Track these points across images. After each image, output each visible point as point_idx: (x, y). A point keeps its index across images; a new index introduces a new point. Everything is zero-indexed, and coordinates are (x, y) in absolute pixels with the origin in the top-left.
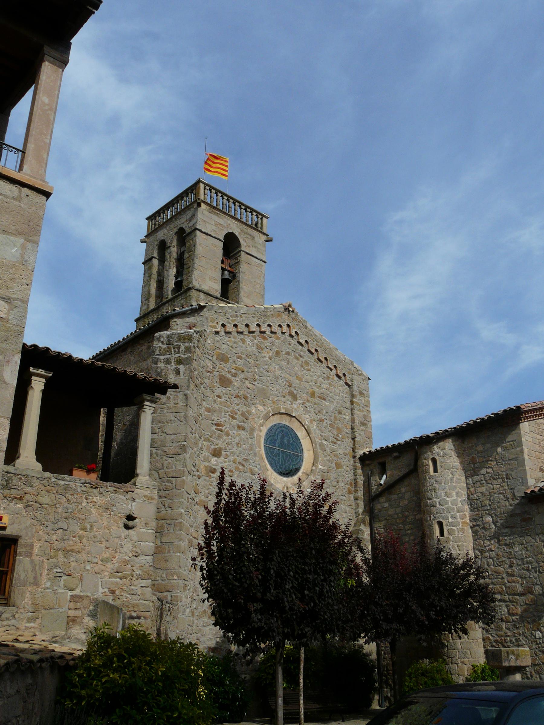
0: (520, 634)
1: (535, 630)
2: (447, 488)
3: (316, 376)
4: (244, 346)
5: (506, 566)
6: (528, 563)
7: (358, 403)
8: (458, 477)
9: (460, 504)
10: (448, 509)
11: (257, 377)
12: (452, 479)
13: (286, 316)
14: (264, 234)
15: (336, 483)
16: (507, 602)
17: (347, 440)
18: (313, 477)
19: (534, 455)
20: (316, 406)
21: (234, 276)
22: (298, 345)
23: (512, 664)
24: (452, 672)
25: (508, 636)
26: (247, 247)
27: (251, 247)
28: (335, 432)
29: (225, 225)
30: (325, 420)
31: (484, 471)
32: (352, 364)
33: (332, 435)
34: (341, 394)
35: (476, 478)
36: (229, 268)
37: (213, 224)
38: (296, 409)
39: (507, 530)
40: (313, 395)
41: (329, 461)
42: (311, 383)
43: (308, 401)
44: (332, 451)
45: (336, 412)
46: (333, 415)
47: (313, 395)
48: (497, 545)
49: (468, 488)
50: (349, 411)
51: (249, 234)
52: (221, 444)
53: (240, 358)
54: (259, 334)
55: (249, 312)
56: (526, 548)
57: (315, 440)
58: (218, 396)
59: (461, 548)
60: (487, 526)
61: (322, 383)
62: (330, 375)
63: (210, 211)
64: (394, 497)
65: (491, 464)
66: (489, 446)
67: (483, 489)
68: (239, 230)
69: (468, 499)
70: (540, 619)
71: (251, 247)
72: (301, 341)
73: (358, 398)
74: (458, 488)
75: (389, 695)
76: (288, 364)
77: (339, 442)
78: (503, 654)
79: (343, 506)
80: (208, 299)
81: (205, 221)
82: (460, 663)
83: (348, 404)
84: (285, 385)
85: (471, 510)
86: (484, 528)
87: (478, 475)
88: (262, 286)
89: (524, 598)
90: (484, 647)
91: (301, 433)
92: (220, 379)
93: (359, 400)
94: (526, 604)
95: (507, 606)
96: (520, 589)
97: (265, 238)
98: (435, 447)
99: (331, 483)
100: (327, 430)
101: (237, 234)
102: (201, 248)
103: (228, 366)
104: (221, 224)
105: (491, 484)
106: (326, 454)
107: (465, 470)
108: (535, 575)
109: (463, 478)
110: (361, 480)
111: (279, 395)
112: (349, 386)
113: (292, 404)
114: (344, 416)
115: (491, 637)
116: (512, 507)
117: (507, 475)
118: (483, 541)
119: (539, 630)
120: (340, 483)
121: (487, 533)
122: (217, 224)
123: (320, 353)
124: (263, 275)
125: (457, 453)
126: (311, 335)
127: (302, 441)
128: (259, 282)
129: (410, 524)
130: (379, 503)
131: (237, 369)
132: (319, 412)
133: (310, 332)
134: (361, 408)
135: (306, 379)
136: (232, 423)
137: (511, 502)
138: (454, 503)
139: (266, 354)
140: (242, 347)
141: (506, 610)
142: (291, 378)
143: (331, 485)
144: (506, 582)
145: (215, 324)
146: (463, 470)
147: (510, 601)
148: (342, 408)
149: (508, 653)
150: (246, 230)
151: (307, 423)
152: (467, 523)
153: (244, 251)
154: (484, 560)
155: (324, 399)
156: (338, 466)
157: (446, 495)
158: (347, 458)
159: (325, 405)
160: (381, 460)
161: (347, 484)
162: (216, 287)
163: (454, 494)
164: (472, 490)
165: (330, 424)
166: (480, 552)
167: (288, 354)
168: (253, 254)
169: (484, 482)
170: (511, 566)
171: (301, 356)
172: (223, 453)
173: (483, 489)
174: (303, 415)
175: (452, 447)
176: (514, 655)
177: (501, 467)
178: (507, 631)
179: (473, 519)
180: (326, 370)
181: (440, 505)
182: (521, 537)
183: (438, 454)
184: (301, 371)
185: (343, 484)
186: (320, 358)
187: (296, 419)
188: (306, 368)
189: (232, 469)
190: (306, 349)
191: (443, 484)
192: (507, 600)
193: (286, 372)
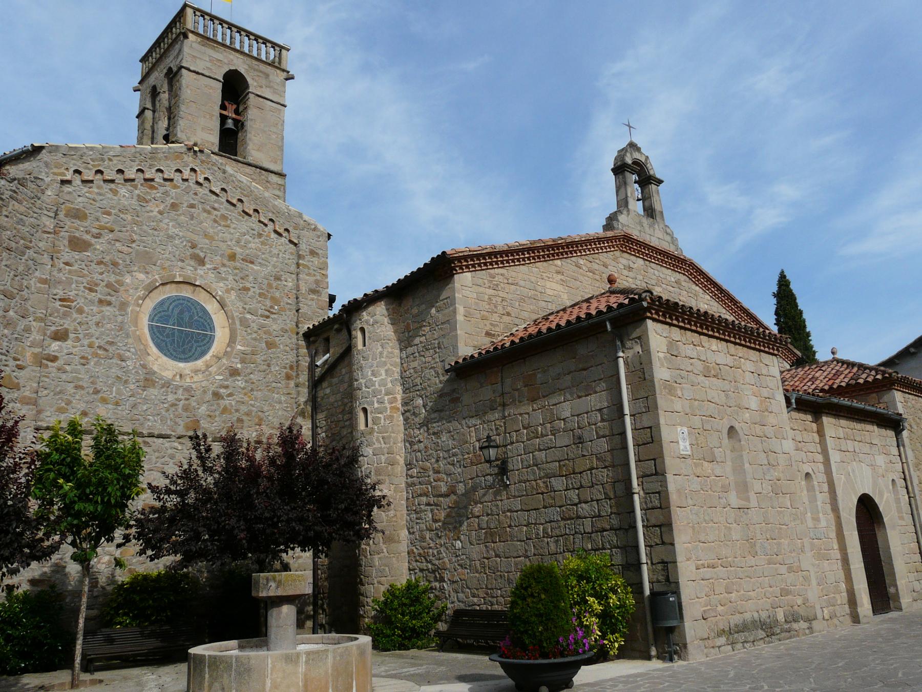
0: (441, 546)
1: (455, 540)
2: (375, 365)
3: (238, 234)
4: (115, 198)
5: (433, 460)
6: (453, 455)
7: (305, 266)
8: (390, 350)
9: (390, 385)
10: (374, 391)
11: (135, 237)
12: (381, 353)
13: (191, 158)
14: (284, 70)
15: (265, 367)
16: (432, 505)
17: (288, 313)
18: (227, 360)
19: (479, 316)
20: (237, 271)
21: (240, 125)
22: (210, 194)
23: (271, 594)
24: (368, 594)
25: (430, 548)
26: (259, 88)
28: (268, 303)
29: (226, 61)
30: (252, 289)
31: (417, 340)
32: (300, 215)
33: (263, 308)
34: (280, 255)
35: (410, 350)
36: (234, 116)
37: (208, 60)
38: (203, 275)
39: (436, 415)
40: (232, 257)
41: (255, 339)
42: (229, 243)
43: (224, 265)
44: (262, 327)
45: (272, 278)
46: (266, 282)
47: (232, 257)
48: (426, 434)
49: (402, 364)
50: (294, 276)
51: (261, 72)
52: (68, 324)
53: (109, 214)
54: (143, 181)
55: (125, 154)
56: (453, 436)
57: (233, 315)
58: (67, 264)
59: (386, 441)
60: (417, 411)
61: (250, 242)
62: (265, 232)
64: (335, 380)
65: (424, 331)
66: (423, 307)
67: (415, 364)
68: (246, 67)
69: (402, 378)
70: (461, 526)
72: (214, 189)
73: (306, 260)
74: (389, 365)
75: (324, 622)
76: (192, 219)
77: (272, 316)
78: (261, 581)
79: (276, 396)
81: (194, 57)
82: (376, 582)
83: (293, 268)
84: (186, 245)
85: (404, 392)
86: (414, 414)
87: (411, 347)
88: (280, 136)
89: (447, 499)
90: (409, 562)
91: (211, 307)
92: (70, 242)
93: (309, 261)
94: (449, 507)
95: (432, 511)
96: (444, 489)
97: (284, 75)
98: (364, 313)
99: (257, 367)
100: (255, 301)
101: (243, 71)
102: (189, 92)
103: (86, 224)
105: (424, 356)
106: (249, 331)
107: (400, 341)
108: (459, 470)
109: (397, 352)
110: (305, 362)
111: (173, 259)
112: (295, 245)
113: (196, 269)
114: (285, 283)
115: (415, 550)
116: (442, 385)
117: (439, 343)
118: (413, 429)
119: (459, 539)
120: (272, 367)
121: (417, 420)
123: (246, 203)
124: (281, 122)
125: (391, 319)
126: (233, 181)
127: (213, 317)
128: (275, 130)
129: (349, 413)
130: (322, 389)
131: (101, 228)
132: (242, 278)
133: (231, 178)
134: (311, 271)
135: (223, 238)
136: (89, 297)
137: (442, 378)
138: (383, 383)
139: (154, 209)
140: (112, 199)
141: (430, 516)
142: (195, 238)
143: (258, 369)
144: (432, 480)
145: (63, 170)
146: (398, 340)
147: (436, 505)
148: (282, 273)
149: (267, 579)
151: (220, 293)
152: (398, 409)
154: (413, 454)
155: (252, 263)
156: (270, 345)
157: (374, 374)
158: (286, 335)
159: (253, 269)
160: (325, 336)
161: (285, 368)
162: (211, 138)
163: (383, 372)
164: (405, 365)
165: (260, 293)
166: (410, 444)
167: (192, 206)
168: (269, 97)
169: (417, 354)
170: (437, 461)
171: (215, 209)
172: (72, 336)
173: (415, 364)
174: (215, 284)
175: (385, 312)
176: (275, 581)
177: (434, 334)
178: (431, 542)
179: (405, 404)
180: (258, 227)
181: (366, 387)
182: (448, 422)
183: (367, 322)
184: (212, 227)
185: (277, 368)
186: (247, 210)
187: (203, 288)
188: (223, 223)
189: (86, 355)
190: (224, 200)
191: (370, 360)
192: (432, 503)
193: (188, 230)
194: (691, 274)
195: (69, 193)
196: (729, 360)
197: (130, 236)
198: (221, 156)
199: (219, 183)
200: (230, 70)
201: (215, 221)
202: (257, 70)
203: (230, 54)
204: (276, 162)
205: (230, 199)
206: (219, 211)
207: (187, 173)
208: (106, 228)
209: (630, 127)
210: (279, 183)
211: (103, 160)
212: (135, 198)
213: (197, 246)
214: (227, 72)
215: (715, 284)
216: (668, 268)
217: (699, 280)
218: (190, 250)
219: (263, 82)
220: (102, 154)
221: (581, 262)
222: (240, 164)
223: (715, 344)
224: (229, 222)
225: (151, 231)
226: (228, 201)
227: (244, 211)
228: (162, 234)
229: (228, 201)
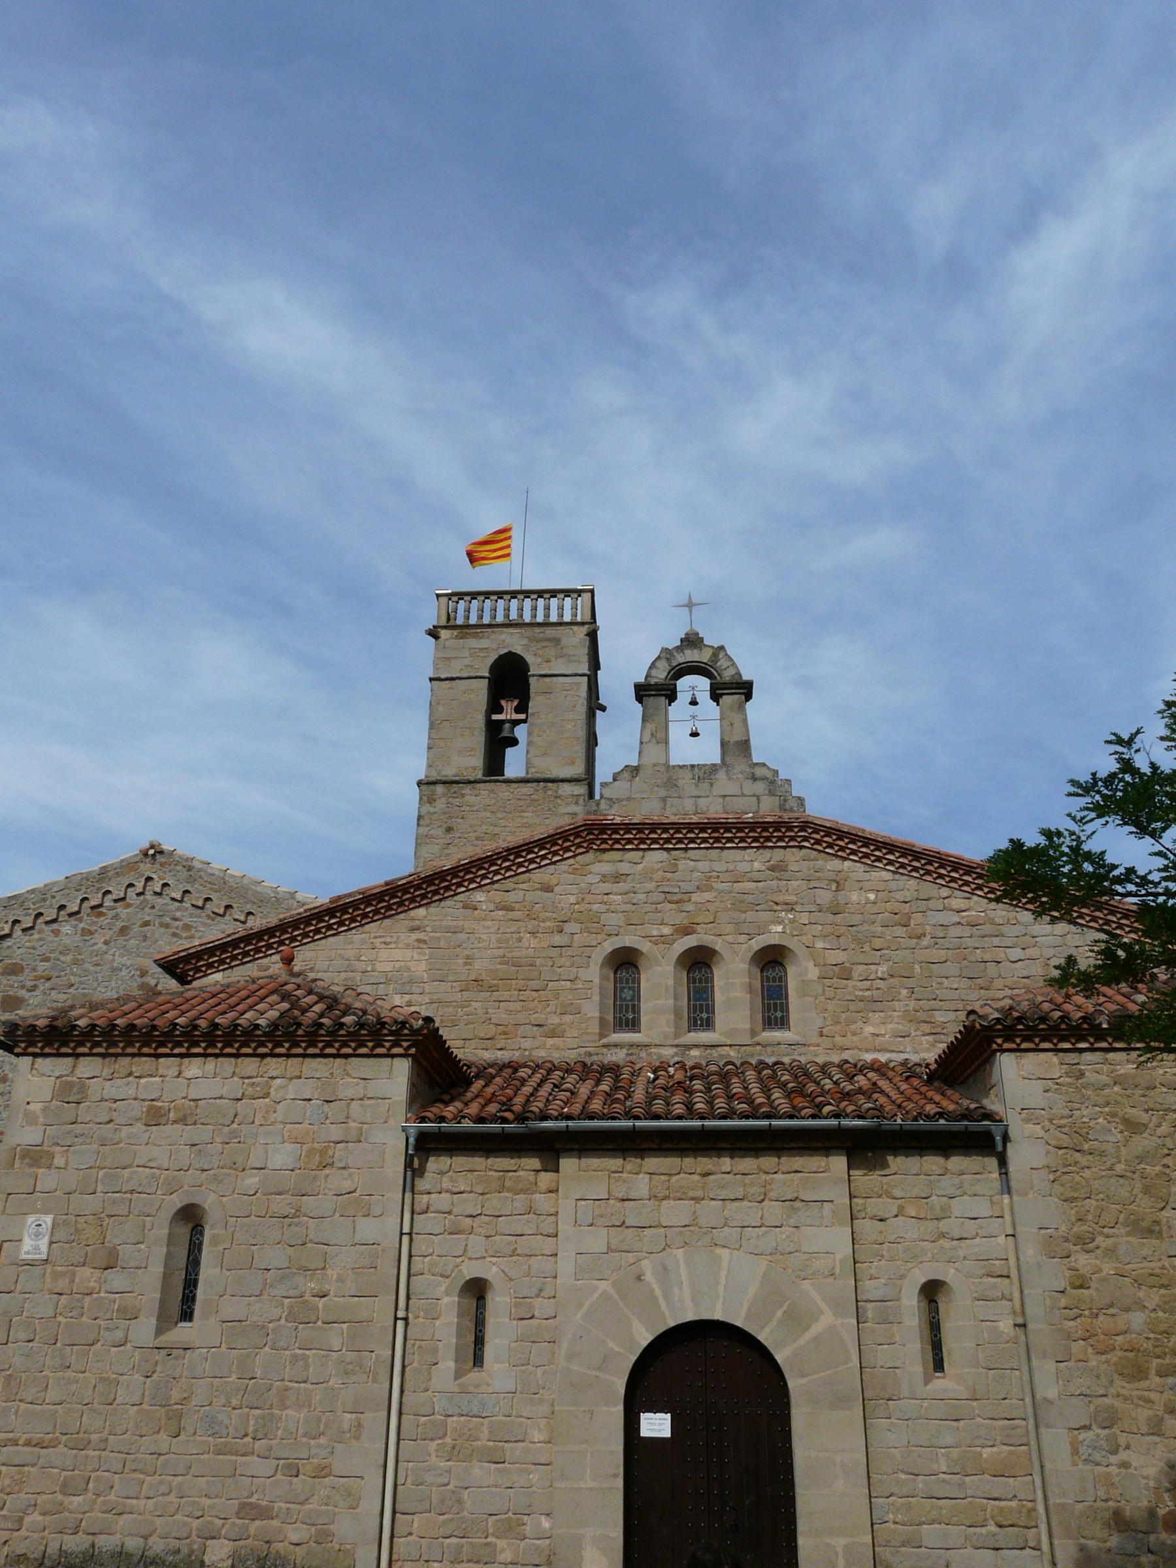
4: (57, 939)
11: (73, 979)
27: (553, 659)
37: (467, 654)
51: (548, 640)
53: (47, 960)
55: (70, 885)
63: (461, 635)
68: (525, 642)
71: (553, 659)
76: (145, 941)
80: (452, 791)
101: (518, 650)
103: (22, 979)
104: (481, 649)
122: (473, 652)
123: (215, 901)
126: (201, 877)
131: (37, 978)
139: (99, 939)
140: (51, 942)
150: (541, 635)
153: (534, 675)
167: (146, 924)
171: (176, 919)
186: (217, 910)
188: (184, 935)
190: (187, 905)
194: (818, 842)
195: (8, 947)
196: (234, 1086)
197: (69, 979)
198: (489, 781)
199: (181, 886)
201: (175, 935)
202: (542, 640)
203: (501, 633)
204: (573, 763)
205: (194, 903)
206: (180, 920)
208: (42, 977)
209: (690, 605)
210: (576, 793)
211: (44, 900)
212: (79, 932)
213: (147, 972)
214: (496, 661)
215: (891, 847)
216: (744, 848)
217: (842, 849)
218: (139, 980)
219: (552, 652)
220: (43, 894)
221: (479, 896)
222: (514, 785)
223: (193, 1068)
224: (193, 931)
225: (92, 969)
226: (193, 905)
227: (214, 913)
228: (105, 968)
229: (193, 905)
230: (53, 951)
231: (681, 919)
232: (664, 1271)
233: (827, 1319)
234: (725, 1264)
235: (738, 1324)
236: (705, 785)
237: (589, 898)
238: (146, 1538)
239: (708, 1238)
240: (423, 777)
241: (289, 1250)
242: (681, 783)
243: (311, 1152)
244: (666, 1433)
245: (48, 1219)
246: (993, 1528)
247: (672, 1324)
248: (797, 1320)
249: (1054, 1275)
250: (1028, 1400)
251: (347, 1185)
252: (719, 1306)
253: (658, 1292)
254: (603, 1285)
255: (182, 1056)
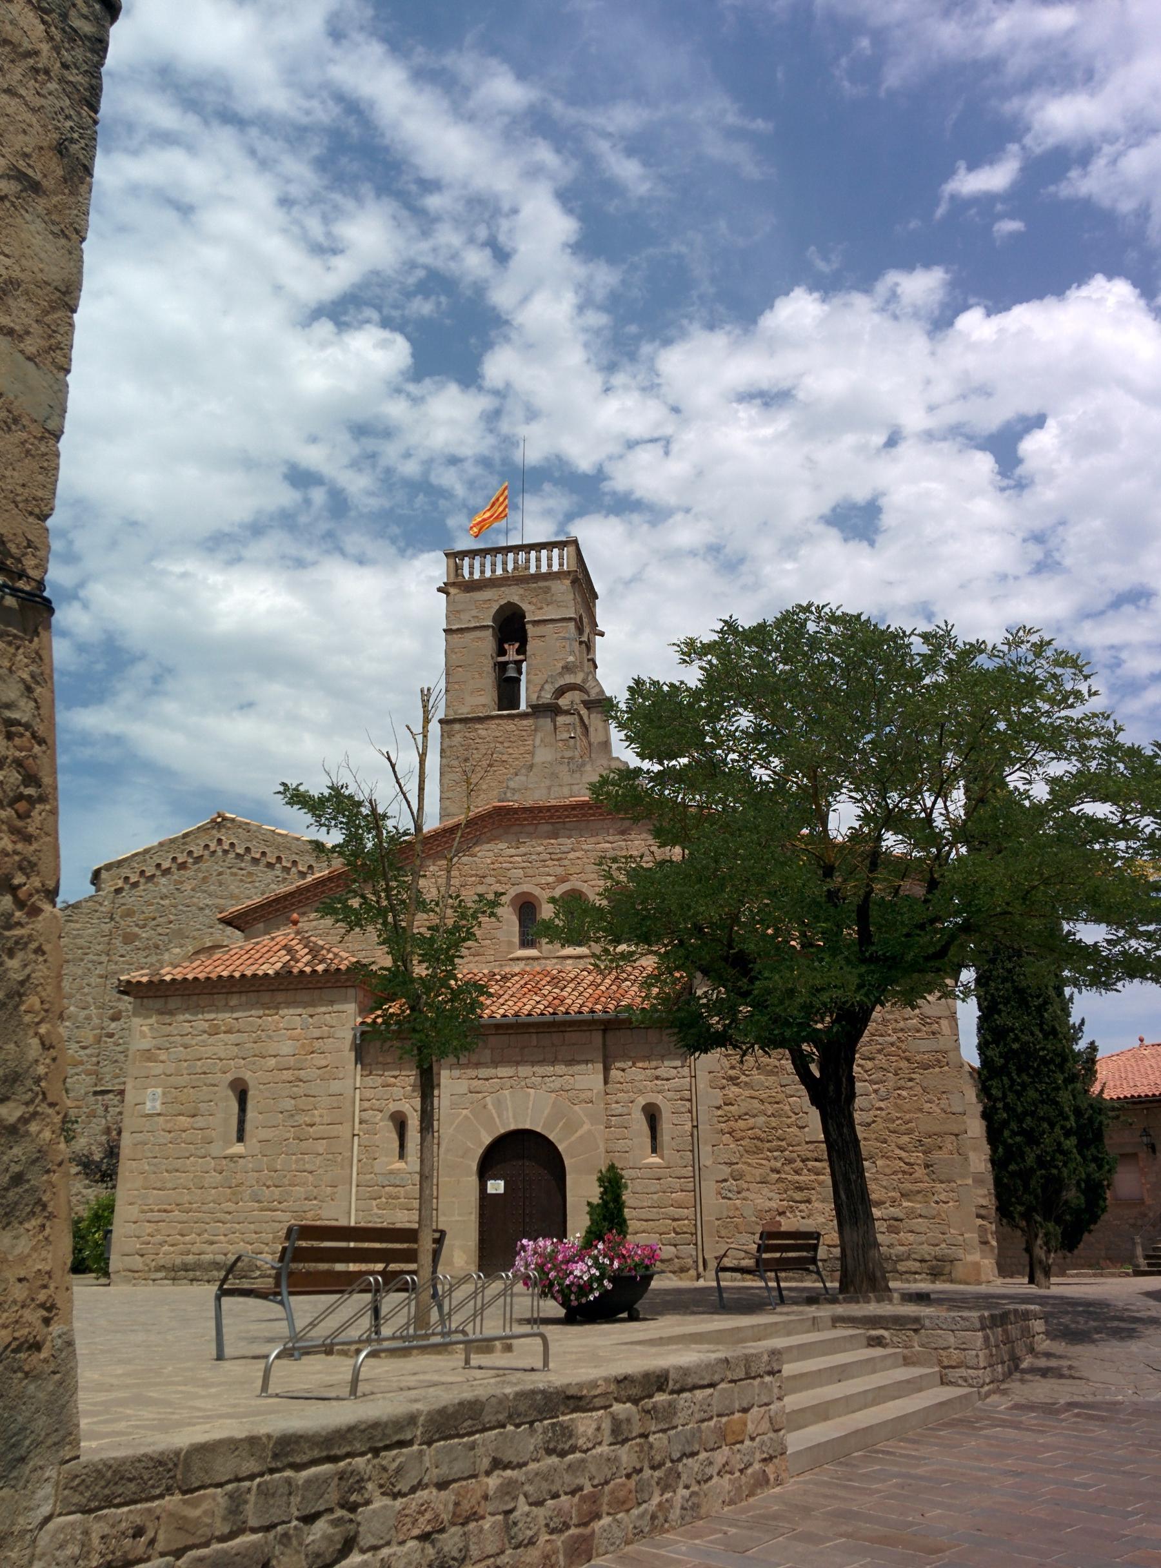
58: (122, 956)
101: (515, 599)
123: (269, 854)
139: (187, 887)
153: (529, 622)
167: (220, 874)
200: (501, 607)
201: (242, 881)
207: (213, 846)
230: (155, 898)
231: (560, 871)
232: (499, 1103)
233: (586, 1127)
234: (532, 1098)
235: (539, 1130)
236: (577, 775)
237: (500, 859)
238: (225, 1255)
239: (523, 1083)
240: (443, 716)
241: (293, 1102)
242: (561, 775)
243: (303, 1045)
244: (501, 1190)
245: (159, 1090)
246: (673, 1235)
247: (502, 1131)
248: (571, 1127)
249: (717, 1097)
250: (697, 1167)
251: (324, 1063)
252: (528, 1121)
253: (495, 1115)
254: (465, 1112)
255: (227, 993)
